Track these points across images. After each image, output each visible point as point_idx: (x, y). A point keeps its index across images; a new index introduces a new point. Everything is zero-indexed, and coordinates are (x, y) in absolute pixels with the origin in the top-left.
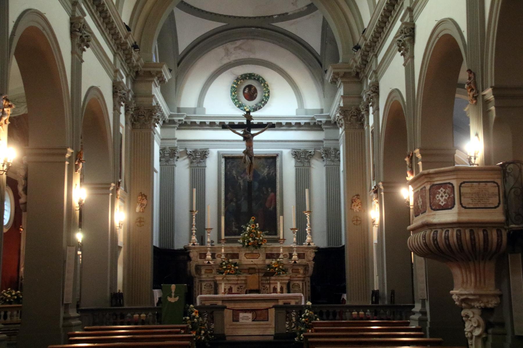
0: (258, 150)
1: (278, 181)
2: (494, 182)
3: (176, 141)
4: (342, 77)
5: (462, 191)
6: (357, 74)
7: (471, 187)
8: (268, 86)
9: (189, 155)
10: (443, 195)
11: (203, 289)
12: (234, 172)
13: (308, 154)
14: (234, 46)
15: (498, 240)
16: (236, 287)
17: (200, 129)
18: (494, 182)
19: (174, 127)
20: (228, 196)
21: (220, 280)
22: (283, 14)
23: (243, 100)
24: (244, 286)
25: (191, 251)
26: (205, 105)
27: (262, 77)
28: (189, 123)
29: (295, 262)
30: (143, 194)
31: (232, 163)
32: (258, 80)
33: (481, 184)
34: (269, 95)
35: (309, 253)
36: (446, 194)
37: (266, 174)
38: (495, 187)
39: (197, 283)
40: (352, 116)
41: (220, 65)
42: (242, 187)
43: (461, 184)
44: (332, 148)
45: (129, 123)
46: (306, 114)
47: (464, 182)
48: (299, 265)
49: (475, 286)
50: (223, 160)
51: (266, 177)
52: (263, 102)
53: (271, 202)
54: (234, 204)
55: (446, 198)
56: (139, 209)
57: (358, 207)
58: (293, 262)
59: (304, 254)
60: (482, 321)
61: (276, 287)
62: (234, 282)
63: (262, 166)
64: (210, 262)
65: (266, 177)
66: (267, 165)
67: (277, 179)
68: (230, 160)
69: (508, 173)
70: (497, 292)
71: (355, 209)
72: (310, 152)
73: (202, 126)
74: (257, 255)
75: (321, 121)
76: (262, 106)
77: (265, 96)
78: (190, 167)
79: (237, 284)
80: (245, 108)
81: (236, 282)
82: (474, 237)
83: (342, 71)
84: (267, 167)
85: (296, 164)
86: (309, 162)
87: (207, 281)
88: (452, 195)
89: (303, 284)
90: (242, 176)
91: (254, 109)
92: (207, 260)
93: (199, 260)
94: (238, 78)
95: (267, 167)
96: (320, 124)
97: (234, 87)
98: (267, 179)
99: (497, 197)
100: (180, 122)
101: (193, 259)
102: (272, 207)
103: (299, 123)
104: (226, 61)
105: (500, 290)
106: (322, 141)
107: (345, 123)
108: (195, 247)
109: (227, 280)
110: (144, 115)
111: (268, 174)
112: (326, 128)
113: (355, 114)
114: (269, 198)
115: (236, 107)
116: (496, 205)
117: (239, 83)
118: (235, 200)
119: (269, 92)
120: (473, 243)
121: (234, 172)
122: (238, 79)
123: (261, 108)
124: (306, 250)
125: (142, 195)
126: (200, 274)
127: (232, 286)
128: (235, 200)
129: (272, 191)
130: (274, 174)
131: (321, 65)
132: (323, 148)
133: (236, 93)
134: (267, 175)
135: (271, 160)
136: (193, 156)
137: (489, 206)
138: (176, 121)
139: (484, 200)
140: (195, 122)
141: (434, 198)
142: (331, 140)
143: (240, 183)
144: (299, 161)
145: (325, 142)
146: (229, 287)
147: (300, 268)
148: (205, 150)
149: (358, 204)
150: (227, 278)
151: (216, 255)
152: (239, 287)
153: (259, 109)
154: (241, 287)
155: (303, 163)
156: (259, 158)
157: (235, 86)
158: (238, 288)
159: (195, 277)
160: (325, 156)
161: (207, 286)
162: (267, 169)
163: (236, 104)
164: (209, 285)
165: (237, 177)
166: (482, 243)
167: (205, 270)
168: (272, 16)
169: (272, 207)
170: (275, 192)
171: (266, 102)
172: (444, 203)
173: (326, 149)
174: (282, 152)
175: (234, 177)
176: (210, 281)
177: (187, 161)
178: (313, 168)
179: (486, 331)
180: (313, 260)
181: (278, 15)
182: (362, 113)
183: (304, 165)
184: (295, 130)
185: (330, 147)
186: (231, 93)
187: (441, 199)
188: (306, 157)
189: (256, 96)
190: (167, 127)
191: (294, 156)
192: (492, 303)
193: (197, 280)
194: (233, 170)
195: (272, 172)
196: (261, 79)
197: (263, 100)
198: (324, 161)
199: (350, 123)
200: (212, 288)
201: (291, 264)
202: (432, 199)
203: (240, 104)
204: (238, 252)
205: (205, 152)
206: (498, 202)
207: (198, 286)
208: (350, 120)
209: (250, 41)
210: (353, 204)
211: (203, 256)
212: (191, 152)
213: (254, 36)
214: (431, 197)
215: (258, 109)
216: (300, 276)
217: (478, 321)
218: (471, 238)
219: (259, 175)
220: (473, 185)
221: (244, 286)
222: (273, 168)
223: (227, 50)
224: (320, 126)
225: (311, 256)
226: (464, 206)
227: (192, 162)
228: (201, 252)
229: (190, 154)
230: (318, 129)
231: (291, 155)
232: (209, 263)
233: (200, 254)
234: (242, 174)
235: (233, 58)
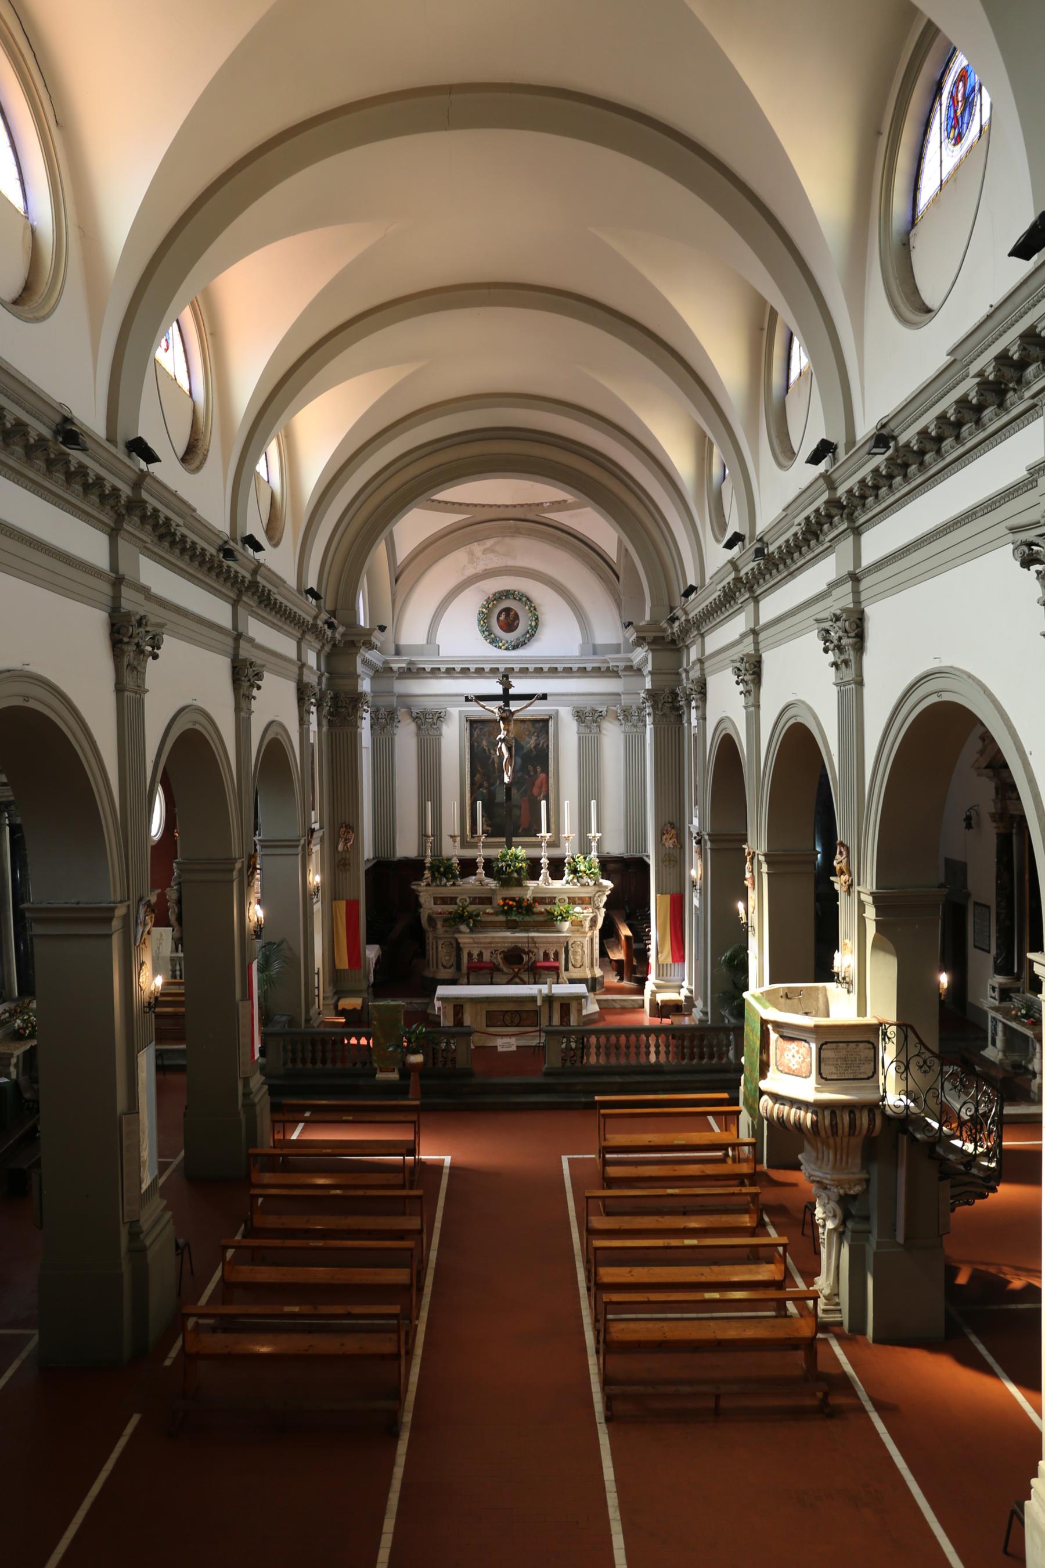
2: (869, 1042)
3: (395, 698)
4: (649, 644)
5: (822, 1056)
6: (673, 642)
7: (837, 1049)
8: (535, 609)
9: (415, 719)
10: (796, 1054)
11: (440, 949)
12: (484, 743)
13: (597, 715)
14: (482, 548)
15: (869, 1125)
17: (431, 678)
18: (869, 1042)
19: (393, 677)
20: (476, 779)
21: (465, 943)
22: (559, 502)
23: (498, 631)
25: (421, 894)
26: (441, 639)
27: (526, 596)
28: (415, 671)
30: (347, 823)
31: (481, 729)
32: (520, 600)
33: (851, 1044)
34: (537, 624)
36: (800, 1055)
37: (532, 746)
38: (870, 1049)
39: (431, 940)
40: (664, 702)
41: (462, 578)
42: (496, 765)
43: (822, 1045)
44: (634, 708)
45: (325, 722)
46: (595, 653)
47: (826, 1043)
49: (834, 1167)
50: (467, 725)
51: (533, 750)
52: (528, 636)
53: (541, 788)
54: (485, 791)
55: (800, 1060)
57: (671, 841)
60: (839, 1212)
61: (547, 951)
62: (484, 945)
65: (533, 750)
66: (534, 732)
67: (549, 753)
68: (479, 724)
69: (889, 1039)
70: (864, 1176)
71: (667, 844)
72: (601, 712)
73: (435, 673)
75: (618, 667)
77: (531, 625)
78: (418, 735)
79: (491, 947)
80: (501, 644)
82: (836, 1123)
83: (650, 635)
84: (536, 734)
85: (578, 730)
86: (599, 726)
87: (445, 938)
88: (809, 1059)
91: (514, 646)
94: (489, 598)
95: (536, 734)
96: (615, 669)
97: (483, 612)
98: (535, 752)
99: (873, 1063)
100: (402, 671)
103: (585, 668)
104: (470, 571)
105: (868, 1173)
106: (619, 695)
107: (655, 714)
110: (345, 707)
111: (536, 747)
112: (624, 676)
113: (670, 700)
114: (538, 782)
115: (486, 643)
116: (870, 1074)
117: (490, 606)
118: (486, 784)
119: (537, 619)
120: (835, 1130)
121: (484, 743)
122: (488, 601)
123: (525, 644)
125: (346, 826)
127: (484, 951)
128: (486, 784)
130: (545, 745)
131: (618, 578)
132: (621, 706)
133: (485, 621)
134: (535, 747)
135: (541, 724)
136: (420, 718)
137: (860, 1076)
138: (395, 669)
139: (852, 1068)
140: (424, 669)
141: (782, 1054)
142: (632, 694)
144: (584, 725)
145: (623, 697)
148: (440, 711)
151: (458, 901)
153: (522, 645)
155: (590, 728)
157: (484, 610)
158: (492, 953)
160: (623, 719)
162: (534, 738)
163: (486, 638)
165: (489, 750)
166: (847, 1129)
168: (542, 503)
170: (546, 770)
171: (533, 635)
172: (796, 1066)
173: (624, 708)
174: (557, 712)
175: (485, 750)
177: (412, 727)
178: (604, 734)
179: (843, 1223)
180: (604, 907)
181: (550, 502)
182: (681, 703)
183: (591, 731)
184: (578, 677)
185: (630, 705)
187: (792, 1058)
188: (595, 718)
189: (518, 624)
191: (576, 718)
192: (856, 1190)
193: (430, 936)
194: (482, 740)
196: (524, 599)
197: (528, 632)
198: (621, 725)
199: (661, 713)
202: (778, 1056)
203: (492, 639)
204: (491, 895)
205: (440, 713)
206: (873, 1070)
207: (433, 944)
208: (662, 708)
209: (508, 540)
210: (664, 837)
212: (418, 713)
213: (516, 533)
214: (778, 1052)
217: (834, 1211)
218: (831, 1125)
219: (522, 747)
220: (838, 1046)
222: (543, 736)
223: (471, 554)
224: (617, 672)
226: (824, 1076)
227: (419, 728)
228: (435, 896)
229: (417, 717)
233: (435, 898)
235: (480, 568)
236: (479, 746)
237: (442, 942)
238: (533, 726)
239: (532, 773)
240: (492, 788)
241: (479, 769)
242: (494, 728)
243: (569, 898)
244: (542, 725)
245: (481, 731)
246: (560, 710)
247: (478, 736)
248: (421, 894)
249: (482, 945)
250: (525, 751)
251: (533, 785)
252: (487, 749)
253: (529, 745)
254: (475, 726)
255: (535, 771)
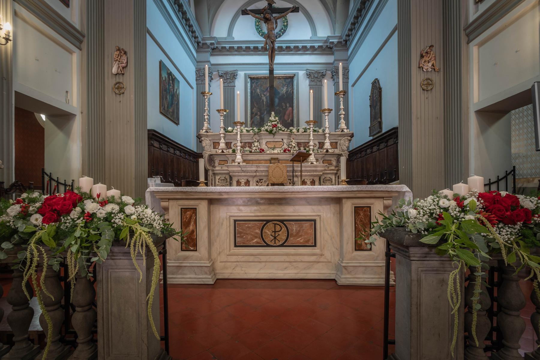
0: (278, 72)
1: (295, 97)
12: (258, 90)
16: (254, 181)
20: (254, 110)
21: (234, 172)
24: (265, 179)
29: (327, 151)
31: (257, 83)
35: (342, 141)
37: (285, 92)
39: (210, 176)
42: (264, 103)
48: (333, 154)
50: (249, 80)
51: (285, 94)
53: (289, 116)
56: (116, 70)
58: (325, 151)
59: (337, 143)
61: (306, 180)
63: (281, 85)
64: (225, 151)
68: (255, 80)
71: (425, 67)
74: (281, 144)
76: (281, 34)
77: (284, 25)
81: (255, 174)
84: (286, 86)
89: (335, 177)
90: (265, 93)
92: (221, 149)
93: (212, 150)
95: (286, 86)
101: (206, 149)
102: (290, 120)
108: (207, 135)
109: (243, 171)
111: (287, 92)
114: (287, 112)
121: (258, 90)
124: (340, 138)
126: (214, 167)
127: (250, 179)
128: (259, 113)
129: (290, 106)
130: (291, 92)
134: (286, 93)
143: (263, 101)
146: (246, 181)
147: (332, 159)
149: (431, 59)
150: (243, 169)
151: (232, 144)
152: (259, 181)
154: (260, 180)
156: (279, 78)
158: (257, 182)
159: (209, 170)
161: (221, 180)
162: (285, 88)
164: (223, 178)
167: (218, 162)
169: (290, 120)
171: (285, 31)
175: (258, 94)
176: (225, 174)
186: (256, 23)
190: (200, 51)
194: (257, 89)
195: (290, 89)
200: (227, 182)
201: (324, 153)
203: (263, 33)
207: (212, 180)
211: (216, 145)
215: (278, 37)
216: (333, 168)
221: (265, 179)
225: (345, 145)
228: (214, 141)
230: (329, 53)
231: (306, 76)
232: (223, 152)
233: (213, 142)
234: (265, 92)
236: (255, 92)
237: (219, 177)
238: (285, 81)
239: (284, 107)
240: (262, 116)
241: (255, 105)
242: (263, 82)
243: (319, 143)
244: (290, 79)
245: (256, 84)
246: (299, 73)
247: (255, 86)
248: (203, 139)
249: (248, 174)
250: (280, 95)
251: (285, 114)
252: (259, 94)
253: (282, 92)
254: (253, 81)
255: (286, 107)
